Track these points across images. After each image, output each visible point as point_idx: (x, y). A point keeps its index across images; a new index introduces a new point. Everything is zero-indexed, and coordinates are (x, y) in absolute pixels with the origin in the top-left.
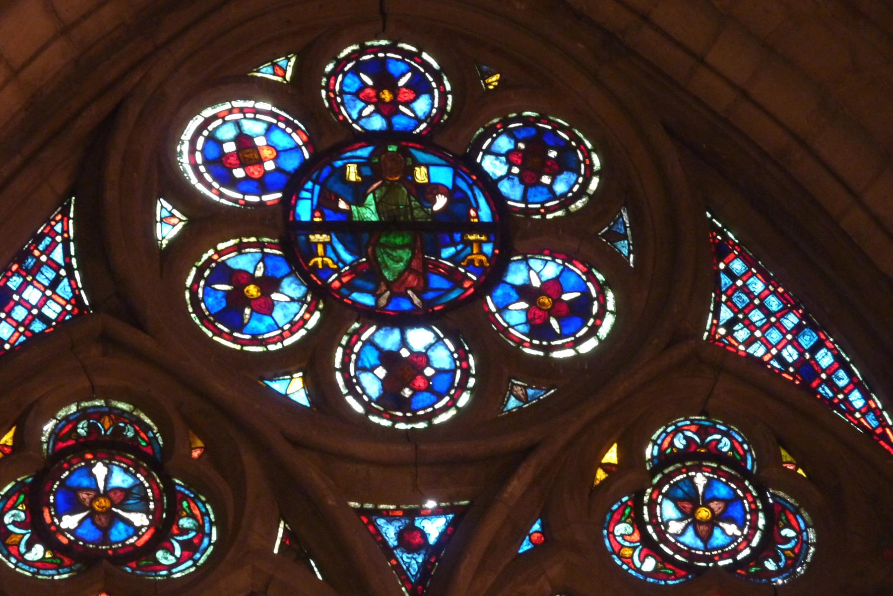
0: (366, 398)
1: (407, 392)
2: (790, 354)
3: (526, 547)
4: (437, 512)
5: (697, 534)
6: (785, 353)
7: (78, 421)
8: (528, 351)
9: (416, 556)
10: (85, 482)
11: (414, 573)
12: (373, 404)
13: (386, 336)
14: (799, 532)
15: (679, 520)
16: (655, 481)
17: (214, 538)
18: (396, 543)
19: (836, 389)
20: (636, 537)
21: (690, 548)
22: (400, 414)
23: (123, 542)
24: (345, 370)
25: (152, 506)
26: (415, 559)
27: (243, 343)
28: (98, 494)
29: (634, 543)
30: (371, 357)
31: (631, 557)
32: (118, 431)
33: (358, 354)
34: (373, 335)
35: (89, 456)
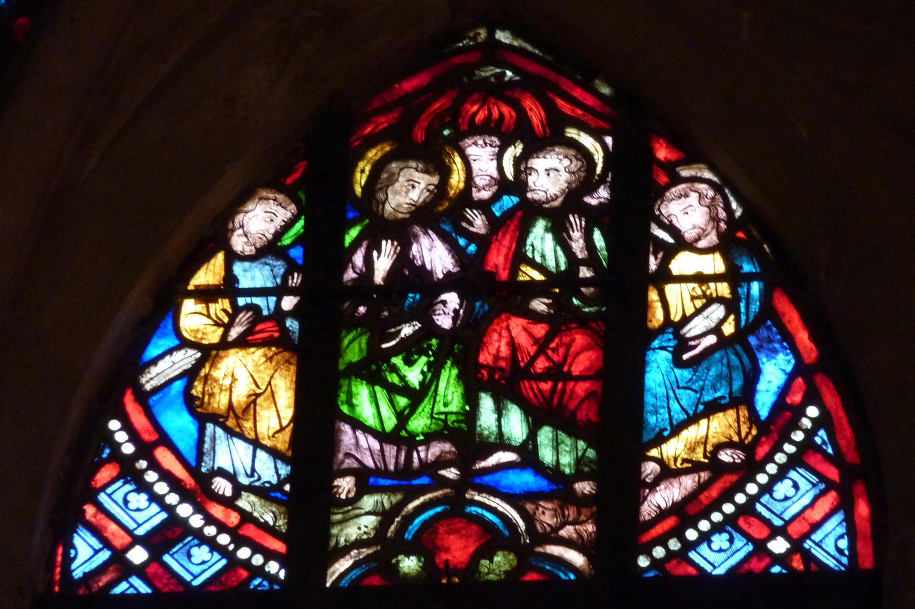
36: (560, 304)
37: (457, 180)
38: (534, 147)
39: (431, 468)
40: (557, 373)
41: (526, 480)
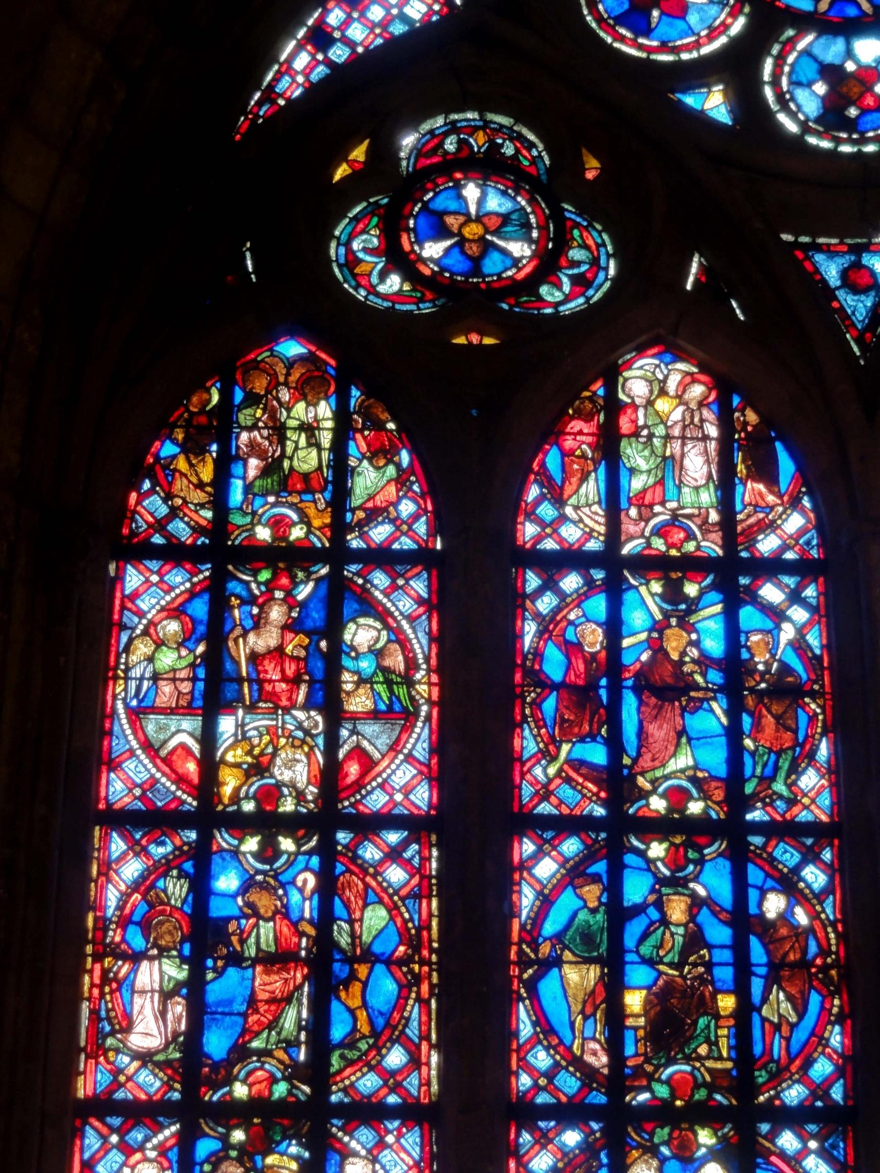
0: (801, 117)
1: (853, 112)
7: (446, 134)
9: (863, 297)
10: (453, 205)
11: (861, 318)
12: (811, 124)
13: (827, 48)
17: (612, 272)
18: (838, 283)
22: (844, 135)
23: (499, 275)
24: (775, 82)
25: (535, 234)
26: (862, 302)
27: (650, 50)
28: (469, 219)
30: (809, 69)
32: (494, 148)
33: (792, 66)
34: (811, 44)
35: (458, 175)
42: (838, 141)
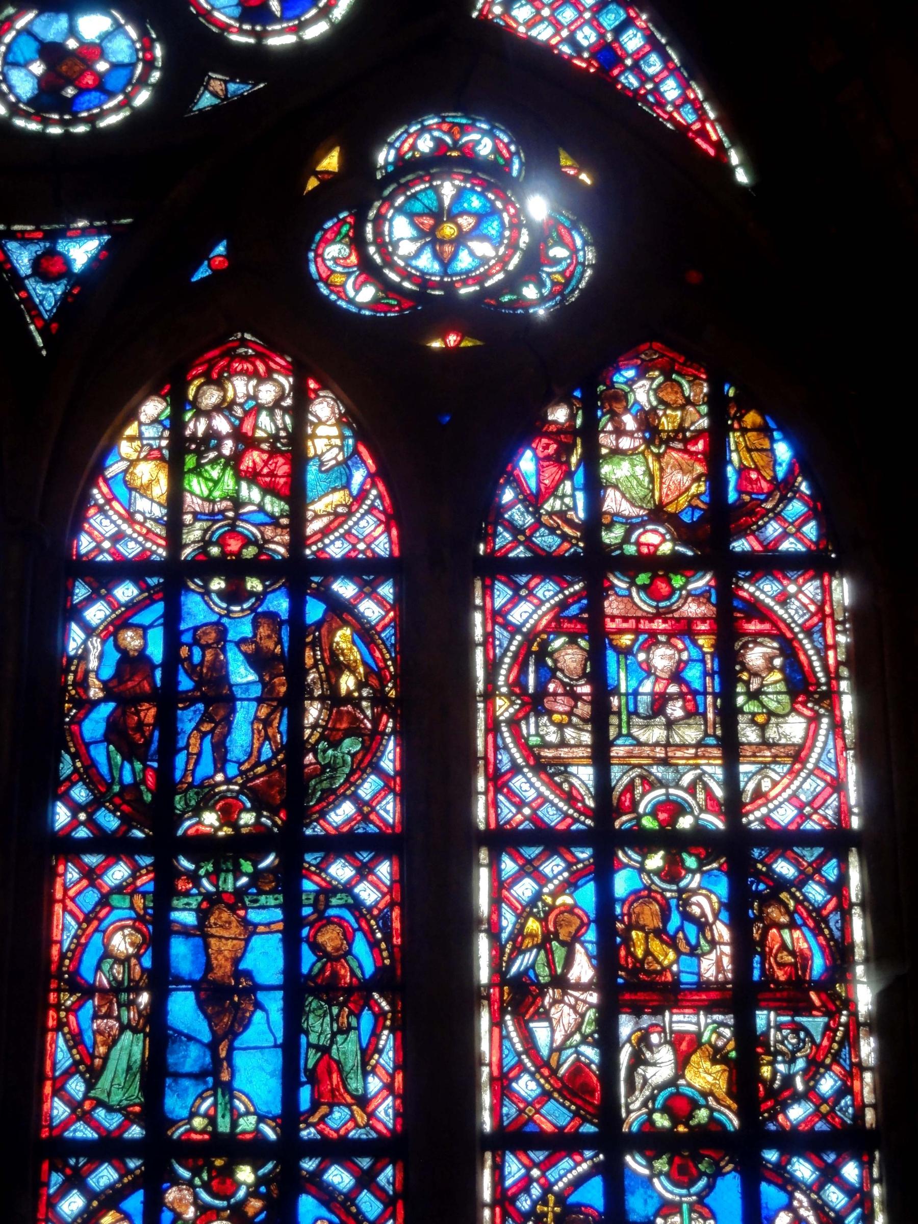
1: (70, 92)
2: (587, 37)
3: (203, 272)
4: (85, 233)
5: (437, 256)
6: (579, 36)
8: (235, 38)
9: (54, 286)
11: (48, 308)
12: (21, 106)
13: (48, 25)
14: (574, 251)
15: (413, 240)
16: (386, 193)
18: (29, 272)
19: (643, 78)
20: (354, 259)
21: (423, 274)
22: (56, 117)
26: (52, 290)
29: (349, 267)
30: (28, 48)
31: (343, 286)
34: (31, 22)
36: (273, 445)
37: (230, 395)
38: (262, 380)
39: (221, 512)
40: (271, 474)
41: (261, 518)
42: (46, 122)
